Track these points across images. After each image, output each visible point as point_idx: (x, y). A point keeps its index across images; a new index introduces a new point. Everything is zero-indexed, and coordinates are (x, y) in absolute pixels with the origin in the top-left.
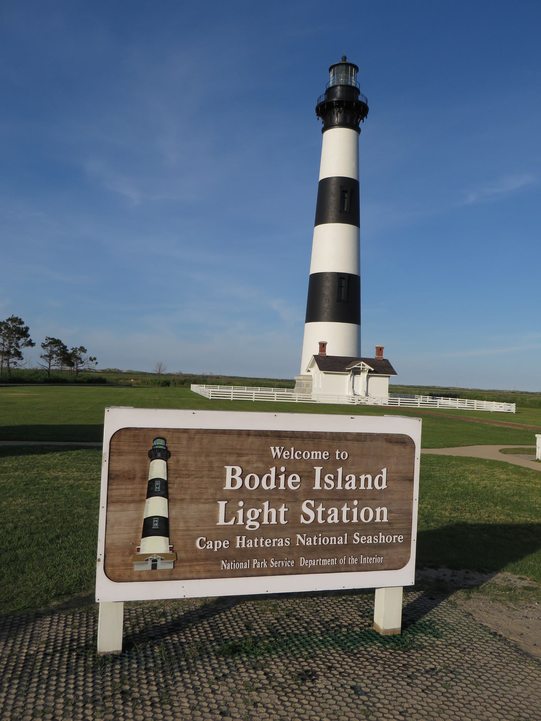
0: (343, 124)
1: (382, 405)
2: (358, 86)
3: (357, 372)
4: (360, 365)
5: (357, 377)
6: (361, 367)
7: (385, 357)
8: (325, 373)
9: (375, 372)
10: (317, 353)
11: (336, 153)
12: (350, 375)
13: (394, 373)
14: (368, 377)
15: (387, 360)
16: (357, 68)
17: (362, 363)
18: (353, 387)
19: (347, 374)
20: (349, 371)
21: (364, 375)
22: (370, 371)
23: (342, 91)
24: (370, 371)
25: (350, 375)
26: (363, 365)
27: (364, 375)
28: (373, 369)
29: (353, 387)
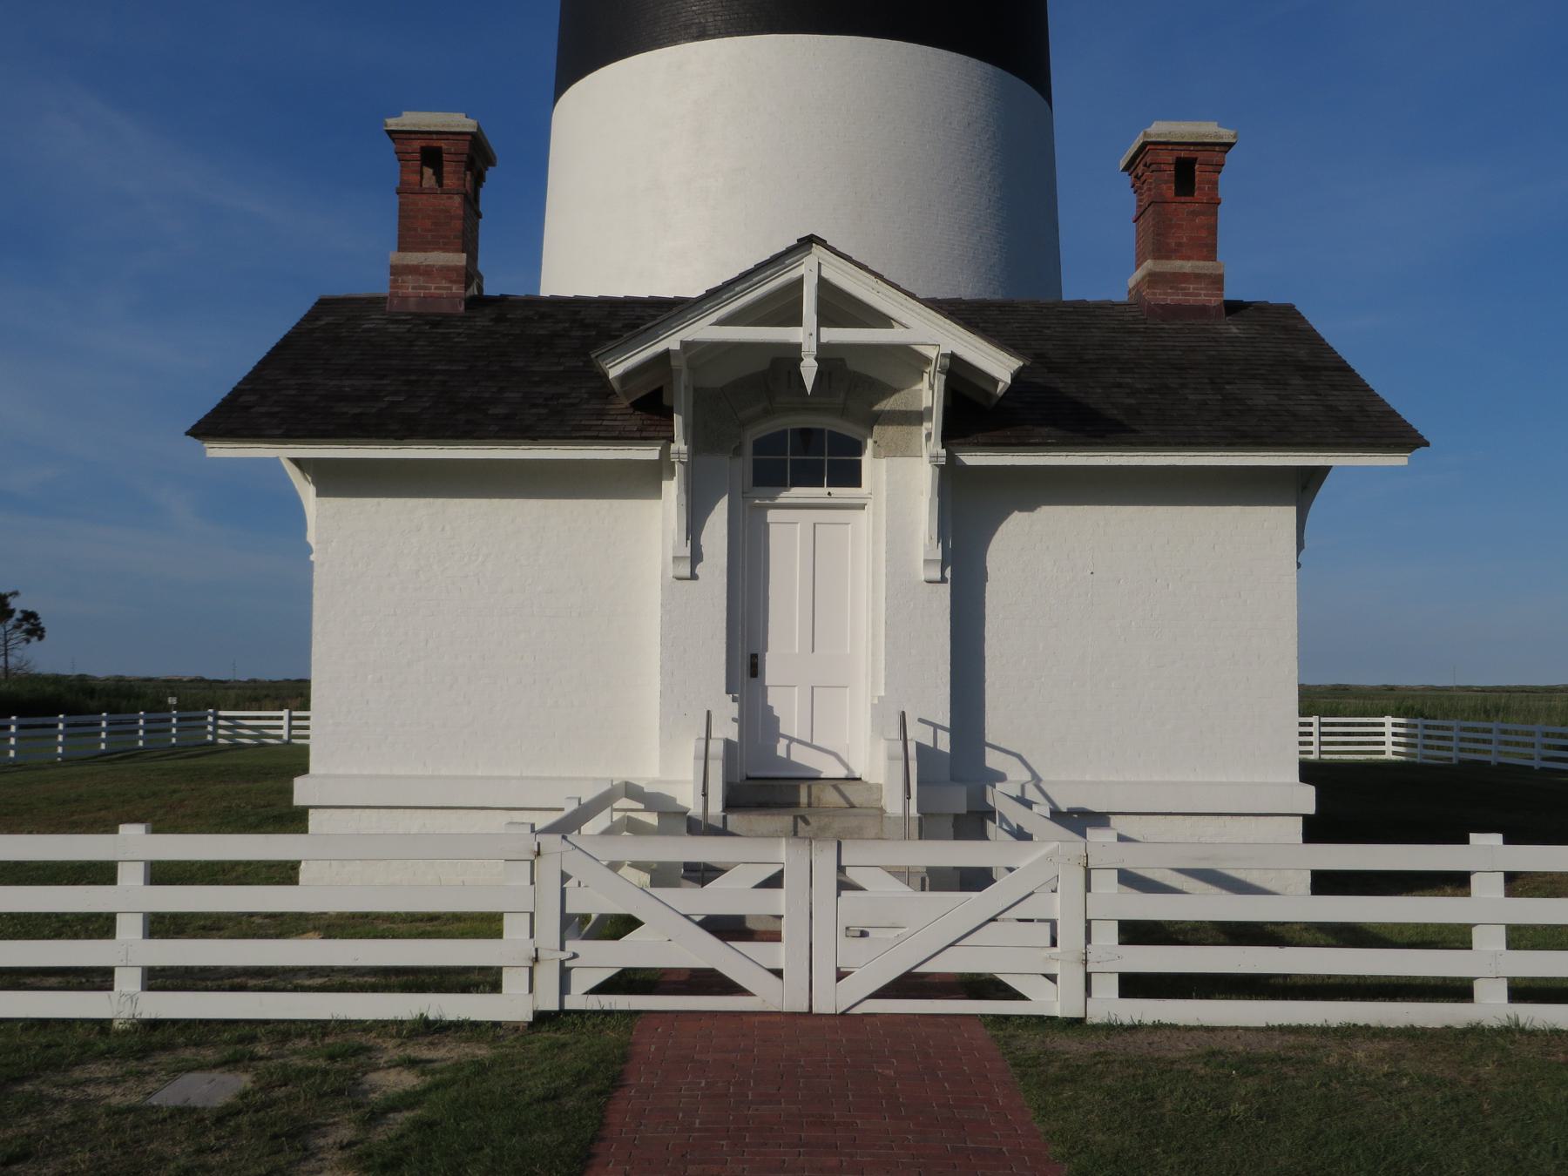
1: (1109, 1006)
6: (805, 335)
7: (1249, 266)
12: (672, 489)
14: (967, 513)
15: (1289, 311)
18: (746, 667)
19: (644, 481)
21: (901, 481)
22: (970, 411)
24: (970, 411)
25: (672, 489)
26: (838, 307)
27: (901, 481)
29: (746, 667)
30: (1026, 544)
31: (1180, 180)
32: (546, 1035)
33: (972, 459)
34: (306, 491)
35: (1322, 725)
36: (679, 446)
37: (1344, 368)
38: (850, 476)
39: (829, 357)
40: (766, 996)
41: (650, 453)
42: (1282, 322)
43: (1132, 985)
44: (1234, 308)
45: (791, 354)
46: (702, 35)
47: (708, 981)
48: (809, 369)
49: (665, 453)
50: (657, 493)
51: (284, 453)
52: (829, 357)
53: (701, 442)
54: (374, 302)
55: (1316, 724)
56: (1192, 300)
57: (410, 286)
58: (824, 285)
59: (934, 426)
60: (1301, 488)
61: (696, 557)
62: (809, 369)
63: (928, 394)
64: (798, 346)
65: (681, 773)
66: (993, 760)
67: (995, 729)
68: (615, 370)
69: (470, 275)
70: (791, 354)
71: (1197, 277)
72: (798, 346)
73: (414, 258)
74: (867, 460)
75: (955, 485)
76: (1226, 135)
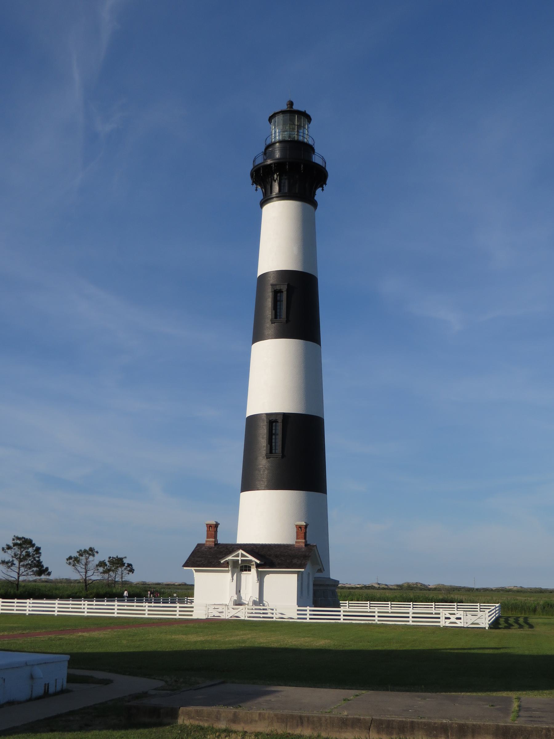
0: (282, 196)
1: (247, 618)
2: (311, 142)
3: (246, 567)
5: (245, 576)
6: (240, 558)
8: (196, 571)
9: (272, 565)
10: (202, 538)
11: (276, 237)
16: (308, 118)
17: (241, 551)
18: (238, 591)
20: (227, 564)
21: (254, 570)
23: (283, 150)
24: (258, 566)
26: (243, 556)
27: (254, 570)
28: (258, 562)
29: (238, 591)
33: (259, 570)
34: (194, 571)
39: (242, 560)
45: (238, 560)
48: (240, 562)
52: (242, 560)
54: (203, 545)
57: (208, 543)
61: (233, 579)
62: (240, 562)
63: (254, 563)
67: (265, 599)
68: (222, 562)
69: (216, 540)
70: (238, 560)
73: (208, 540)
75: (257, 572)
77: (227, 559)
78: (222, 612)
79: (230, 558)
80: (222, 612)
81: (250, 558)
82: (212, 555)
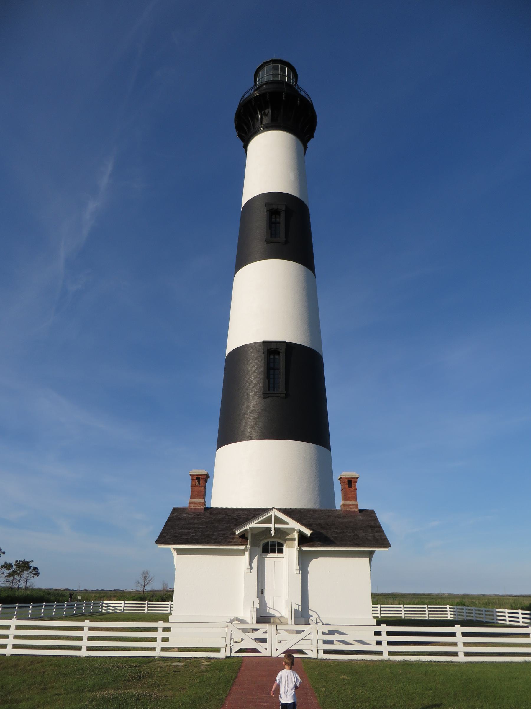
1: (322, 656)
3: (271, 545)
4: (268, 521)
5: (271, 561)
6: (272, 526)
8: (180, 552)
10: (184, 500)
12: (247, 554)
13: (382, 541)
14: (304, 560)
15: (373, 512)
18: (261, 592)
21: (291, 551)
22: (303, 540)
24: (303, 540)
25: (247, 554)
26: (278, 520)
27: (291, 551)
28: (308, 532)
29: (261, 592)
30: (317, 566)
31: (349, 483)
32: (228, 660)
34: (175, 553)
35: (404, 608)
36: (248, 546)
37: (380, 527)
38: (281, 551)
39: (276, 530)
40: (265, 653)
41: (243, 547)
42: (370, 515)
43: (326, 652)
44: (361, 511)
45: (270, 529)
46: (251, 439)
47: (255, 651)
48: (273, 532)
49: (246, 547)
50: (244, 555)
51: (171, 547)
52: (276, 530)
53: (252, 545)
54: (184, 509)
55: (403, 608)
56: (352, 510)
57: (193, 507)
58: (276, 517)
59: (297, 542)
60: (370, 554)
61: (251, 568)
62: (273, 532)
63: (296, 535)
64: (271, 528)
65: (248, 615)
66: (310, 613)
68: (237, 533)
69: (205, 503)
71: (353, 505)
72: (271, 528)
74: (284, 548)
75: (301, 554)
76: (357, 475)
77: (248, 527)
78: (264, 641)
79: (253, 524)
80: (264, 641)
81: (292, 524)
82: (202, 527)
